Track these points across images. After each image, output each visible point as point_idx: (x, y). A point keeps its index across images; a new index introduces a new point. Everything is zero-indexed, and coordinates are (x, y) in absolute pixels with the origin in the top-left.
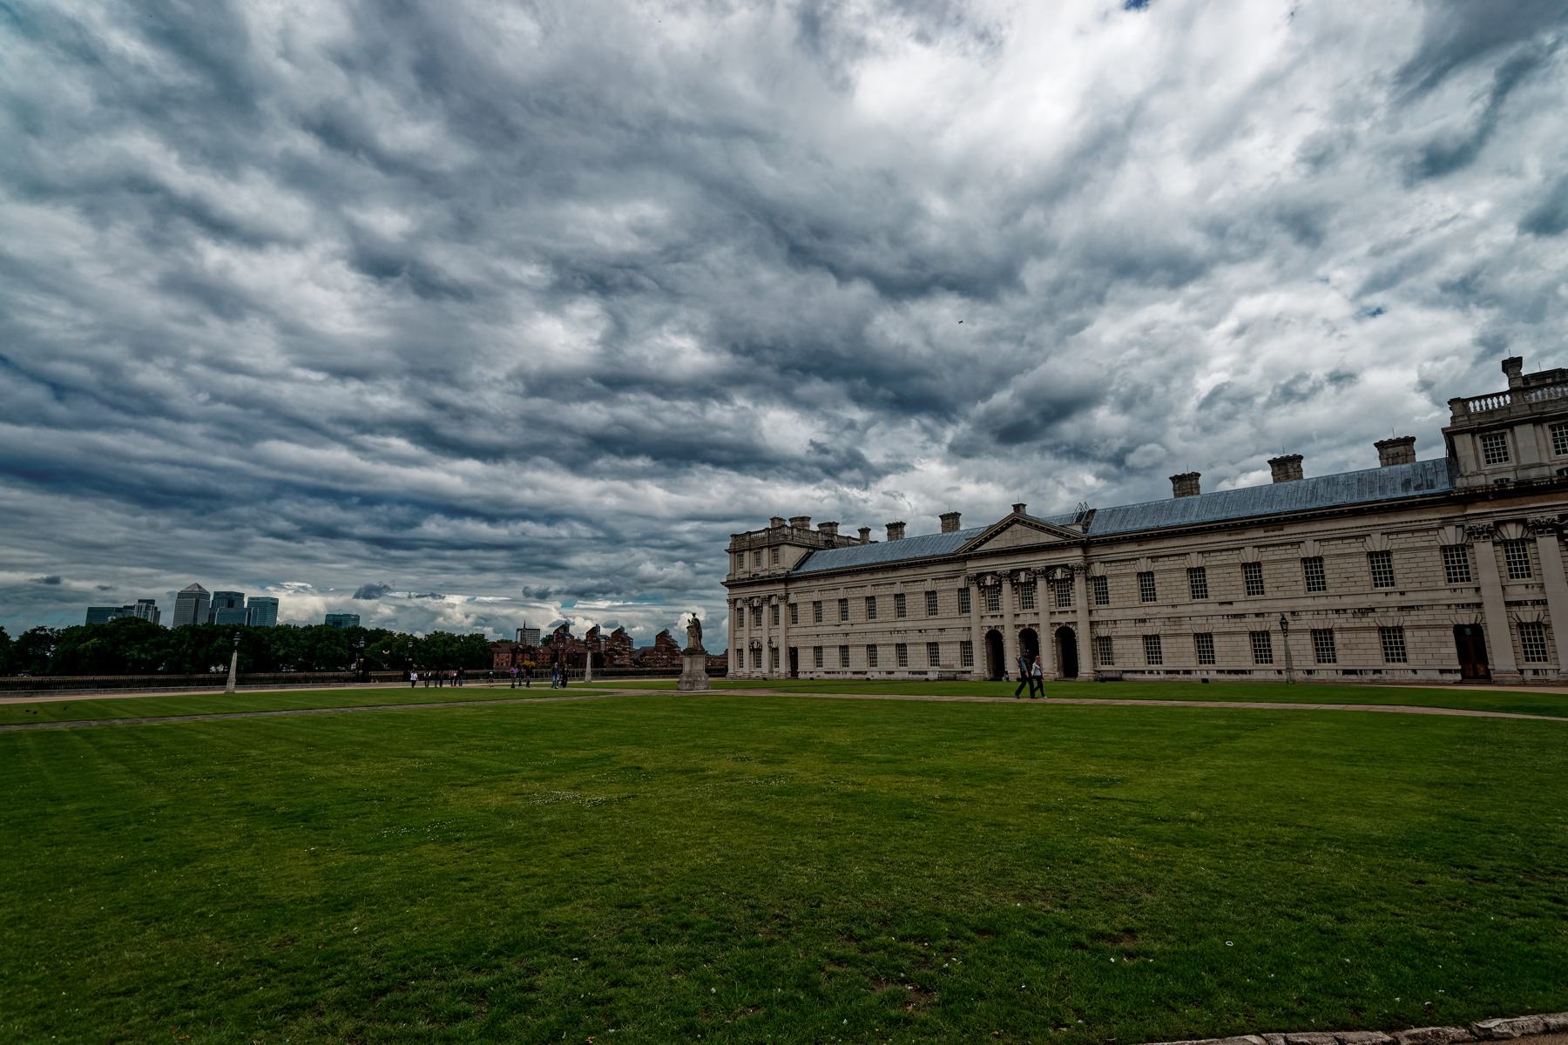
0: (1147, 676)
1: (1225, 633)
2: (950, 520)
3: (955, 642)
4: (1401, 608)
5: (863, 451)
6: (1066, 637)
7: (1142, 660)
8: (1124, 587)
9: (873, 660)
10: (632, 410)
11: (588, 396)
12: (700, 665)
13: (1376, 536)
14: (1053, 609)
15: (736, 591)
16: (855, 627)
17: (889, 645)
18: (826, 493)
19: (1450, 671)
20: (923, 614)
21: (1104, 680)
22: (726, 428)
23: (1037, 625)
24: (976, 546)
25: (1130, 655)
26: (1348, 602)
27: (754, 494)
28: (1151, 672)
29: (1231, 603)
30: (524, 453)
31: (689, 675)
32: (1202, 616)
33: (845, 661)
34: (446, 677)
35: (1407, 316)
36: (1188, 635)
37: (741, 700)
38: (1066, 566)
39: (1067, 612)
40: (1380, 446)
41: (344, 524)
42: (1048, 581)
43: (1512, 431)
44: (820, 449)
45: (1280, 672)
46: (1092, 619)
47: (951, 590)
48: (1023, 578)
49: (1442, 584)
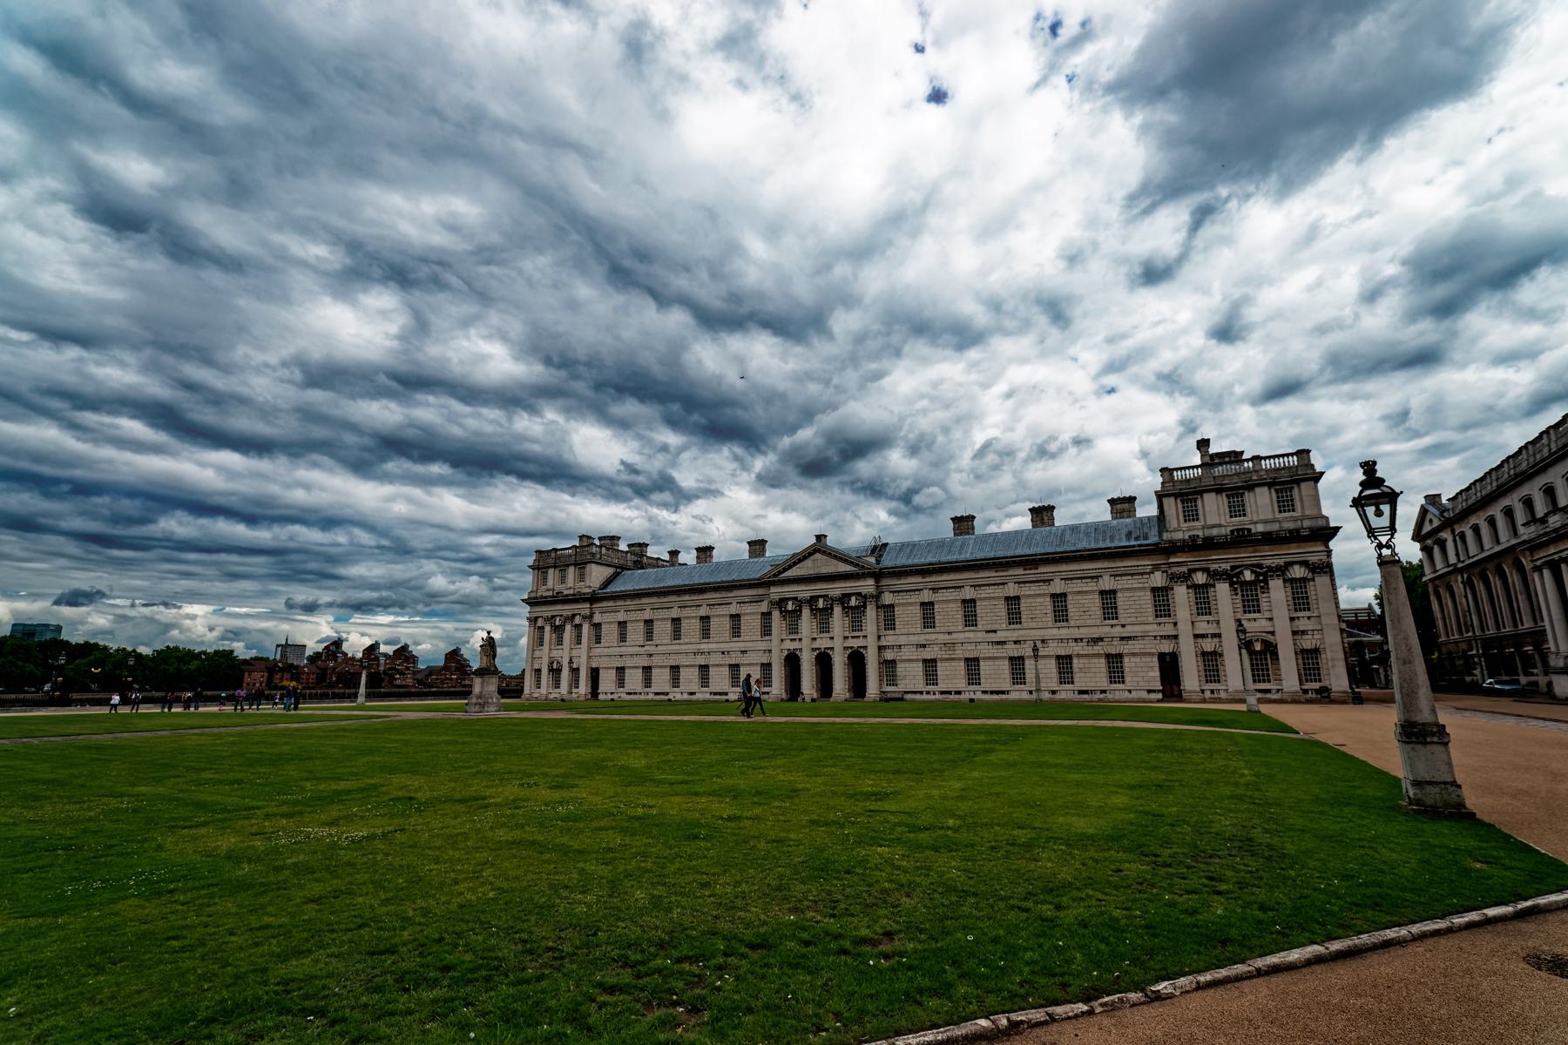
0: (925, 697)
1: (990, 658)
2: (757, 546)
3: (756, 664)
4: (1122, 639)
5: (675, 474)
6: (856, 660)
7: (921, 682)
8: (907, 615)
9: (675, 681)
10: (429, 412)
11: (379, 393)
12: (492, 686)
13: (1106, 578)
14: (847, 634)
15: (537, 609)
16: (660, 648)
17: (692, 666)
18: (635, 513)
19: (1154, 691)
20: (727, 635)
21: (887, 700)
22: (534, 441)
23: (832, 649)
24: (780, 573)
26: (1083, 632)
27: (561, 510)
28: (928, 693)
29: (995, 631)
30: (297, 449)
31: (479, 697)
32: (972, 641)
33: (648, 682)
34: (178, 700)
35: (1133, 397)
36: (960, 659)
37: (533, 722)
38: (859, 594)
40: (1112, 501)
41: (46, 515)
42: (844, 608)
43: (1202, 497)
44: (631, 469)
45: (1031, 692)
46: (881, 644)
47: (752, 614)
48: (821, 603)
49: (1151, 619)
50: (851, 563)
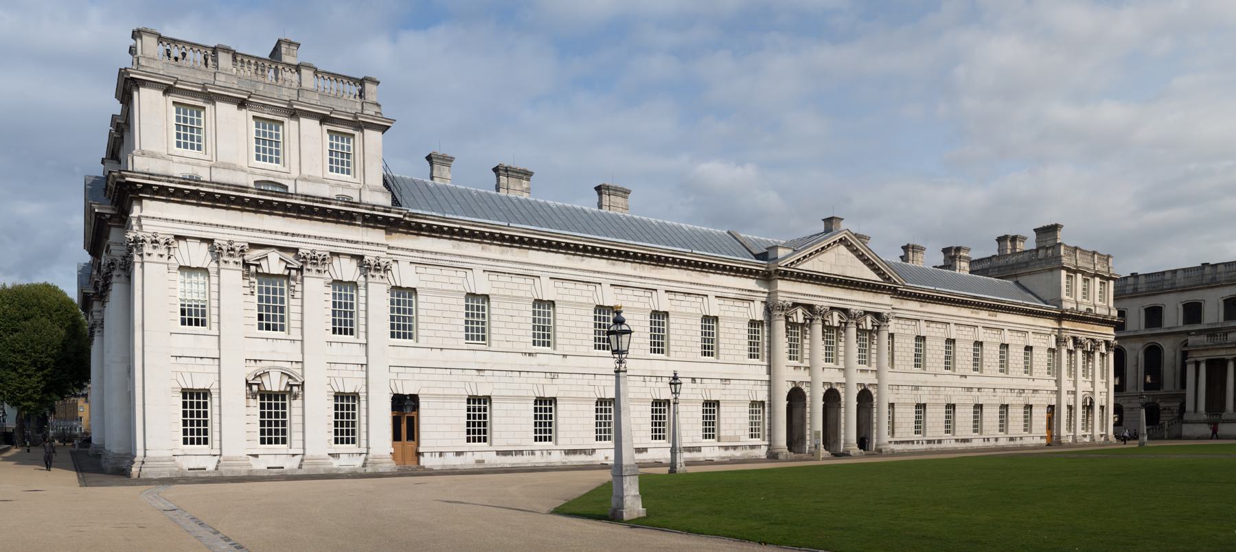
25: (905, 427)
26: (1016, 384)
39: (868, 370)
50: (876, 270)
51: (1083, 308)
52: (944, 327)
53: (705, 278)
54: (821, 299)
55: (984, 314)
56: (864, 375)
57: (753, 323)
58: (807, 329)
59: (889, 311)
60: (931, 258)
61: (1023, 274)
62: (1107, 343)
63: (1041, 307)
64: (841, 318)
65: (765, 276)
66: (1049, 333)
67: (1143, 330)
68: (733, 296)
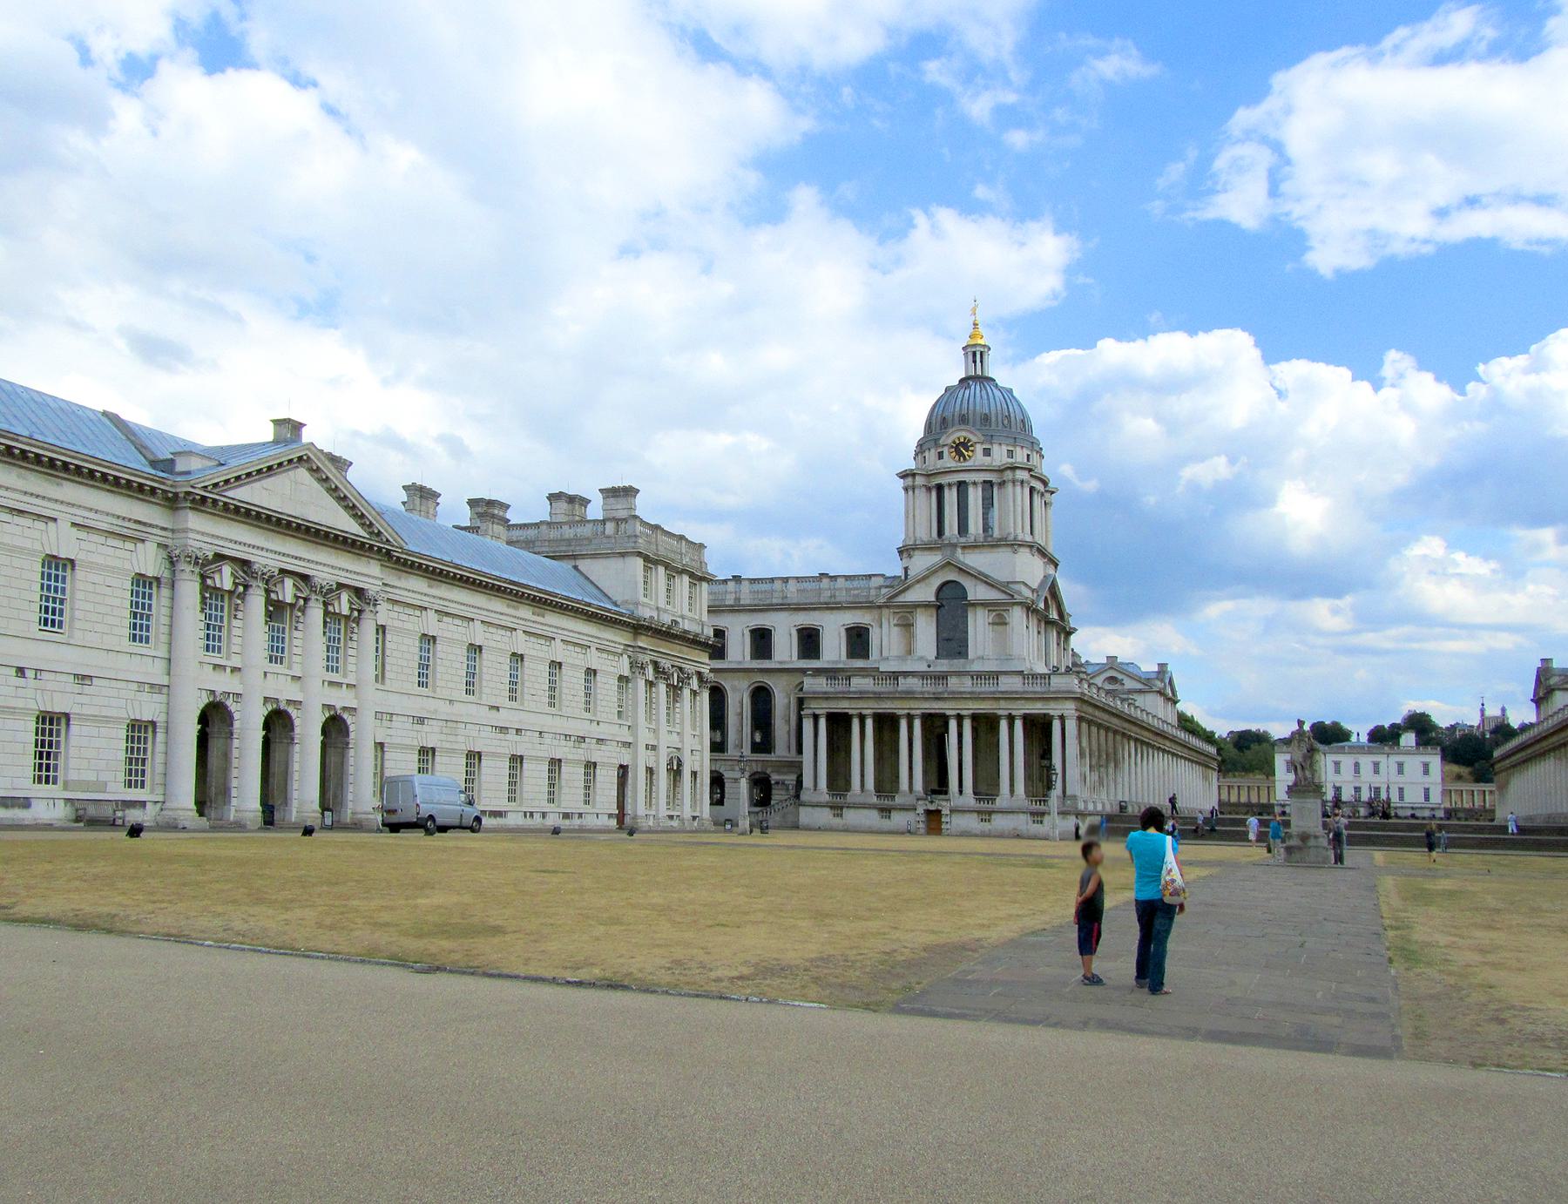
3: (117, 720)
39: (339, 685)
43: (656, 569)
50: (359, 517)
51: (666, 619)
52: (465, 624)
53: (55, 487)
54: (264, 553)
55: (525, 612)
56: (334, 691)
57: (141, 580)
58: (239, 602)
59: (378, 589)
60: (454, 510)
61: (583, 557)
62: (699, 674)
63: (609, 611)
64: (298, 589)
65: (168, 499)
66: (620, 651)
67: (749, 663)
68: (105, 526)
